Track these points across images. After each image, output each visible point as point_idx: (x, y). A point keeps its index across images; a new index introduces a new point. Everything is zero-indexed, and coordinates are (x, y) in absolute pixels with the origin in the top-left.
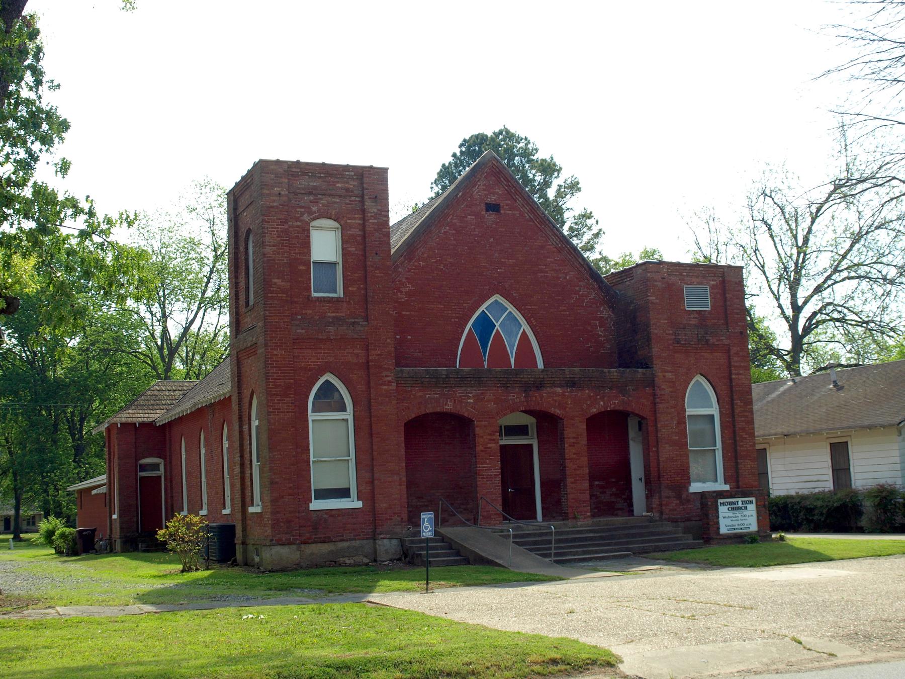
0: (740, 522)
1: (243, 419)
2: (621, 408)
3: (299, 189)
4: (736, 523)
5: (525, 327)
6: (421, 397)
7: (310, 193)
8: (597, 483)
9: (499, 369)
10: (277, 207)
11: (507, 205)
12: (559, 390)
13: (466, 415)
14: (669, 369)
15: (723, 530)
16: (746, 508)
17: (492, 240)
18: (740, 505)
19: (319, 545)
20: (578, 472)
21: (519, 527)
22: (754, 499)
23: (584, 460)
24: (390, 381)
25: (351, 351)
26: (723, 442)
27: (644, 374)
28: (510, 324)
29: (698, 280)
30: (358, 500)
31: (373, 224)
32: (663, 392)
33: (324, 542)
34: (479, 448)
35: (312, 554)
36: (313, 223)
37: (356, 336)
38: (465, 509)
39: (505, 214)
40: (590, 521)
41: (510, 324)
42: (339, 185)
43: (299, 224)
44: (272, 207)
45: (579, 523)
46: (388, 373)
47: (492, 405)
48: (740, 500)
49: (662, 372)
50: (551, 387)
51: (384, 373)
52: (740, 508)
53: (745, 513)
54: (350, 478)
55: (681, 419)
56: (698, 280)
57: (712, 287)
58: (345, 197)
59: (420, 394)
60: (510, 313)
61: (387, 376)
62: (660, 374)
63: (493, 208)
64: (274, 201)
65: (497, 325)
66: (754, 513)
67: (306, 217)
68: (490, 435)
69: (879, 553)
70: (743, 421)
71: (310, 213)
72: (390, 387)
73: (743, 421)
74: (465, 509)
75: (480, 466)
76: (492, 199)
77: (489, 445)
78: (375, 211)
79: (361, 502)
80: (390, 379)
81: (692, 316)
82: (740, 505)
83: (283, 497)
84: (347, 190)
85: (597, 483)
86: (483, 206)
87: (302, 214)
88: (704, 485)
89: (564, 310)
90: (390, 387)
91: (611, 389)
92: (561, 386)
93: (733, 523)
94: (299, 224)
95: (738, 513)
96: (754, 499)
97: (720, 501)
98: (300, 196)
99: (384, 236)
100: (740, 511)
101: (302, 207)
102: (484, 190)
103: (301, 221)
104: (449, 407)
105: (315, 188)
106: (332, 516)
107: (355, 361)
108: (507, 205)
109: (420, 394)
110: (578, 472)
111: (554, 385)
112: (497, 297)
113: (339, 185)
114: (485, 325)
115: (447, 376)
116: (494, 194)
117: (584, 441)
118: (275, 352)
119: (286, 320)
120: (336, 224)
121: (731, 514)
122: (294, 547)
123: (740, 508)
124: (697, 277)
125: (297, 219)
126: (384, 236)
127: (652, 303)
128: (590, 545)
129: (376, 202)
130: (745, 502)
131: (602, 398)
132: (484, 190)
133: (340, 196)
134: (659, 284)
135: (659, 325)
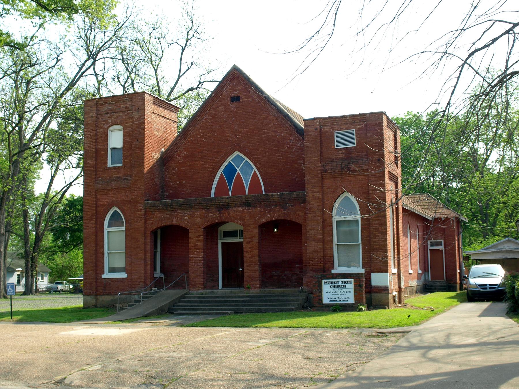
0: (339, 296)
1: (6, 236)
2: (283, 218)
3: (103, 112)
4: (336, 297)
5: (255, 169)
6: (159, 217)
7: (108, 113)
8: (298, 265)
9: (201, 198)
10: (91, 123)
11: (244, 96)
12: (240, 209)
13: (184, 226)
14: (317, 190)
15: (326, 301)
16: (345, 286)
17: (234, 119)
18: (340, 284)
19: (106, 296)
20: (252, 259)
21: (212, 292)
22: (352, 280)
23: (256, 252)
24: (141, 209)
25: (124, 194)
26: (362, 239)
27: (297, 195)
28: (245, 168)
29: (346, 126)
30: (363, 268)
31: (136, 124)
32: (311, 206)
33: (108, 295)
34: (191, 245)
35: (103, 301)
36: (111, 128)
37: (125, 186)
38: (212, 280)
39: (243, 102)
40: (258, 291)
41: (245, 168)
42: (122, 106)
43: (102, 130)
44: (89, 124)
45: (251, 291)
46: (140, 205)
47: (199, 220)
48: (340, 280)
49: (313, 193)
50: (235, 207)
51: (139, 205)
52: (339, 286)
53: (344, 290)
54: (121, 262)
55: (327, 224)
56: (346, 126)
57: (358, 130)
58: (125, 111)
59: (159, 215)
60: (246, 161)
61: (140, 206)
62: (310, 195)
63: (236, 99)
64: (90, 120)
65: (238, 169)
66: (352, 291)
67: (106, 126)
68: (197, 237)
69: (315, 325)
70: (376, 224)
71: (108, 123)
72: (141, 213)
73: (376, 224)
74: (212, 280)
75: (191, 256)
76: (235, 94)
77: (197, 243)
78: (138, 116)
79: (364, 270)
80: (141, 208)
81: (340, 152)
82: (340, 284)
83: (88, 271)
84: (126, 108)
85: (298, 265)
86: (229, 99)
87: (104, 125)
88: (349, 269)
89: (279, 156)
90: (141, 213)
91: (276, 206)
92: (241, 206)
93: (334, 296)
94: (102, 130)
95: (338, 290)
96: (352, 280)
97: (323, 281)
98: (103, 115)
99: (142, 129)
100: (340, 289)
101: (104, 121)
102: (230, 89)
103: (103, 128)
104: (174, 222)
105: (111, 110)
106: (113, 281)
107: (126, 199)
108: (244, 96)
109: (159, 215)
110: (252, 259)
111: (236, 206)
112: (237, 153)
113: (122, 106)
114: (231, 171)
115: (172, 205)
116: (236, 90)
117: (256, 240)
118: (87, 198)
119: (93, 181)
120: (121, 127)
121: (332, 290)
122: (93, 297)
123: (339, 286)
124: (346, 124)
125: (101, 128)
126: (142, 129)
127: (307, 147)
128: (224, 306)
129: (138, 112)
130: (345, 282)
131: (269, 213)
132: (230, 89)
133: (122, 112)
134: (313, 133)
135: (312, 162)
